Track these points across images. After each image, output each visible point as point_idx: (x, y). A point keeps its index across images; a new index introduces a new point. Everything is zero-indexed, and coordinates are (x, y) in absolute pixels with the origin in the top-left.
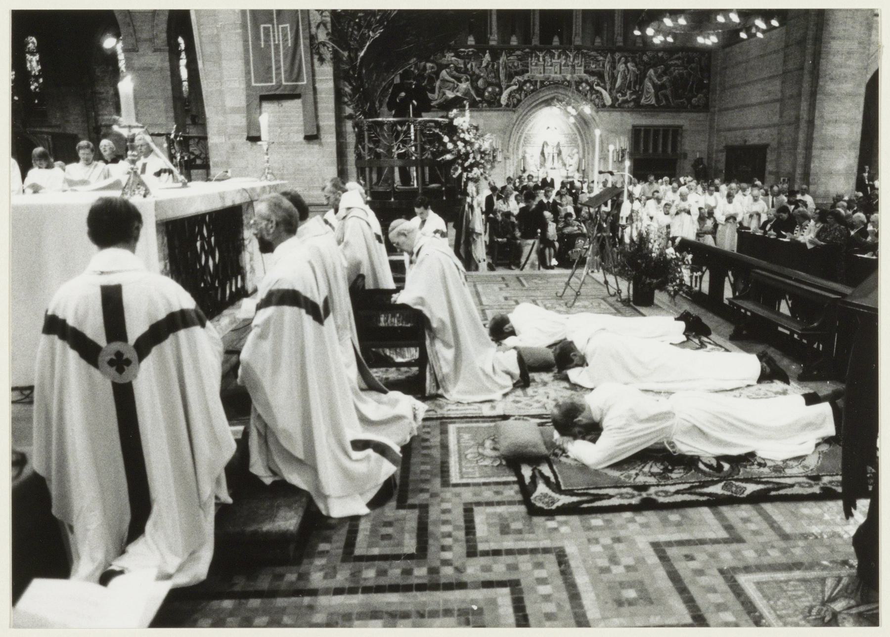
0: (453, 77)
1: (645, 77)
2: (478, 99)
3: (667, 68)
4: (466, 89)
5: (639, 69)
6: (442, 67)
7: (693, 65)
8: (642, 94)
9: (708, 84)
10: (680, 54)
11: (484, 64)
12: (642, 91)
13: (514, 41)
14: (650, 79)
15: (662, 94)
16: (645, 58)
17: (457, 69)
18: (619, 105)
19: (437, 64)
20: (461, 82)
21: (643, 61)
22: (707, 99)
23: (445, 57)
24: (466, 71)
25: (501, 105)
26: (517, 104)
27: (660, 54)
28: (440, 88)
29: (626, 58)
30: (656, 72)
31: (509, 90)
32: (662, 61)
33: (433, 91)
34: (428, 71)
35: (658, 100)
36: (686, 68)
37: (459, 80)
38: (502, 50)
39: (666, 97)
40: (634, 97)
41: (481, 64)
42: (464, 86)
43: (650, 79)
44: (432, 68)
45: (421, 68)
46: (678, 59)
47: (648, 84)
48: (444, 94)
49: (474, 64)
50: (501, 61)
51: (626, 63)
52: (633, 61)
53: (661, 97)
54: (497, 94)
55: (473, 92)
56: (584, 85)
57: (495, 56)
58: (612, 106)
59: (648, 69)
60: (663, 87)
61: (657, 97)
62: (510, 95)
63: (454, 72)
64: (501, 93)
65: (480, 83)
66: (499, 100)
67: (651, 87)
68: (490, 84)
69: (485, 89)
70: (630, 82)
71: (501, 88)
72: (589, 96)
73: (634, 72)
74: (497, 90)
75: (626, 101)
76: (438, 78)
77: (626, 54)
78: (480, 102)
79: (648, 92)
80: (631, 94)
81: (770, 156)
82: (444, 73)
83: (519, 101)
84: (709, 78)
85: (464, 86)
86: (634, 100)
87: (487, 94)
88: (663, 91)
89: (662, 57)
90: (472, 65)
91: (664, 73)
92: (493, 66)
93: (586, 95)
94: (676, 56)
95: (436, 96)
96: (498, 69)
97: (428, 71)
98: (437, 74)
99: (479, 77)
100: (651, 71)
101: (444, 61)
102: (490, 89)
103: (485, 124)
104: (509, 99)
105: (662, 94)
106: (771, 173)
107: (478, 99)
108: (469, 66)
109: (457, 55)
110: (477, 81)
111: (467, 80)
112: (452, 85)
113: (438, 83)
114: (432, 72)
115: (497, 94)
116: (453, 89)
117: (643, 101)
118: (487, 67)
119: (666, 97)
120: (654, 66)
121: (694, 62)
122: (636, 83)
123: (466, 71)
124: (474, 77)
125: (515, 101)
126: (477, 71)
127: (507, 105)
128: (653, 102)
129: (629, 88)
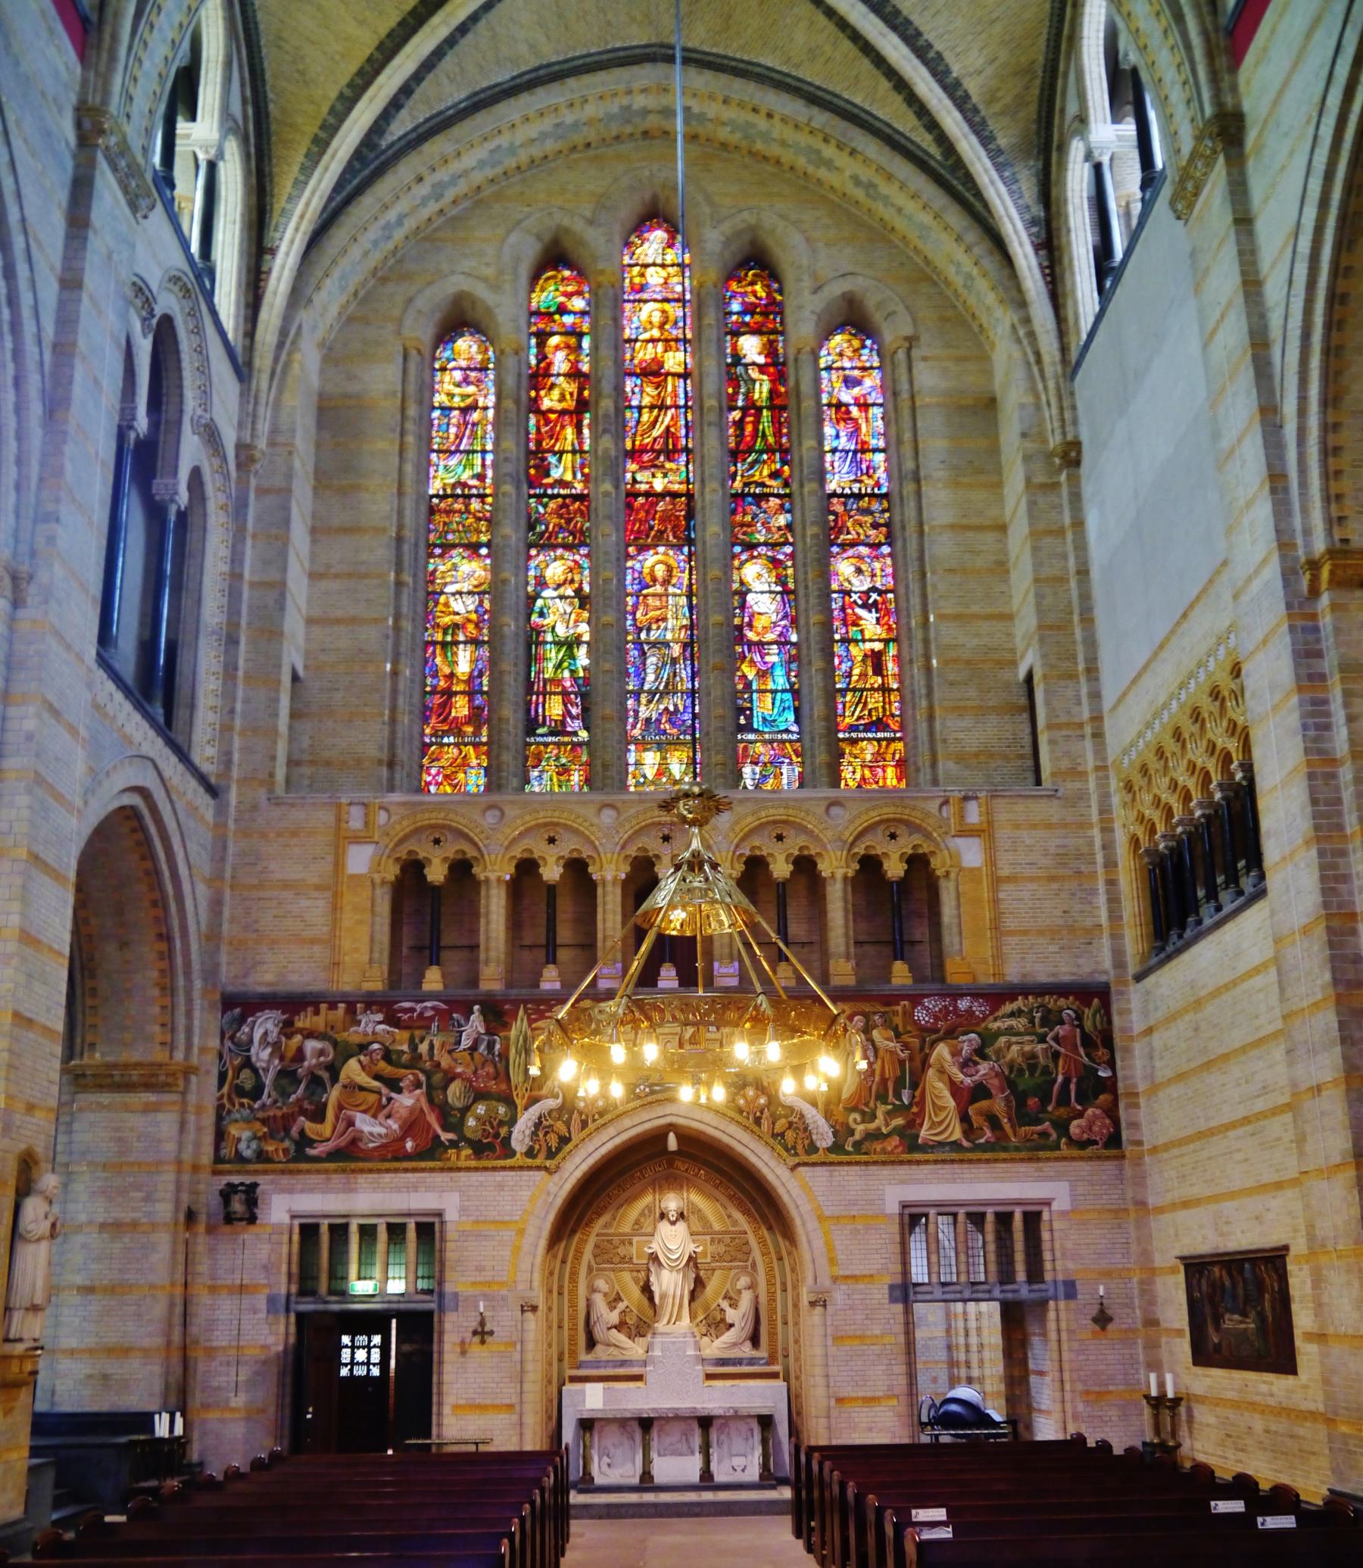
0: (377, 1077)
1: (925, 1064)
2: (445, 1136)
3: (988, 1039)
4: (412, 1110)
5: (906, 1046)
6: (345, 1052)
7: (1061, 1030)
8: (921, 1113)
9: (1114, 1078)
10: (1020, 1003)
11: (466, 1043)
12: (922, 1104)
13: (550, 980)
14: (942, 1071)
15: (980, 1113)
16: (920, 1015)
17: (387, 1055)
18: (857, 1145)
19: (335, 1044)
20: (399, 1091)
21: (916, 1023)
22: (1116, 1123)
23: (359, 1023)
24: (415, 1062)
25: (512, 1154)
26: (559, 1149)
27: (963, 1004)
28: (340, 1107)
29: (865, 1015)
30: (955, 1053)
31: (535, 1111)
32: (969, 1022)
33: (318, 1116)
34: (310, 1061)
35: (969, 1129)
36: (1042, 1039)
37: (394, 1085)
38: (516, 1003)
39: (994, 1122)
40: (899, 1121)
41: (459, 1043)
42: (406, 1101)
43: (942, 1071)
44: (321, 1053)
45: (290, 1054)
46: (1015, 1014)
47: (937, 1088)
48: (351, 1123)
49: (437, 1044)
50: (513, 1033)
51: (867, 1030)
52: (888, 1024)
53: (977, 1121)
54: (501, 1123)
55: (432, 1119)
56: (751, 1092)
57: (497, 1014)
58: (837, 1148)
59: (933, 1044)
60: (980, 1092)
61: (965, 1118)
62: (538, 1125)
63: (382, 1064)
64: (513, 1121)
65: (455, 1093)
66: (507, 1139)
67: (947, 1093)
68: (480, 1096)
69: (465, 1110)
70: (884, 1081)
71: (508, 1101)
72: (765, 1124)
73: (892, 1053)
74: (502, 1110)
75: (875, 1136)
76: (335, 1079)
77: (867, 1008)
78: (453, 1144)
79: (938, 1109)
80: (890, 1115)
81: (1299, 1281)
82: (353, 1069)
83: (564, 1140)
84: (1111, 1064)
85: (406, 1101)
86: (899, 1131)
87: (471, 1122)
88: (983, 1104)
89: (970, 1012)
90: (433, 1043)
91: (981, 1053)
92: (490, 1046)
93: (758, 1121)
94: (1008, 1008)
95: (326, 1129)
96: (504, 1056)
97: (310, 1061)
98: (334, 1070)
99: (450, 1077)
100: (942, 1051)
101: (353, 1035)
102: (481, 1109)
103: (463, 1210)
104: (534, 1134)
105: (980, 1113)
106: (1309, 1337)
107: (445, 1136)
108: (423, 1048)
109: (392, 1020)
110: (445, 1088)
111: (417, 1085)
112: (372, 1098)
113: (334, 1095)
114: (319, 1065)
115: (501, 1123)
116: (375, 1111)
117: (924, 1133)
118: (474, 1048)
119: (994, 1122)
120: (950, 1034)
121: (1062, 1023)
122: (899, 1084)
123: (415, 1062)
124: (437, 1078)
125: (554, 1144)
126: (445, 1061)
127: (530, 1153)
128: (957, 1135)
129: (882, 1097)
